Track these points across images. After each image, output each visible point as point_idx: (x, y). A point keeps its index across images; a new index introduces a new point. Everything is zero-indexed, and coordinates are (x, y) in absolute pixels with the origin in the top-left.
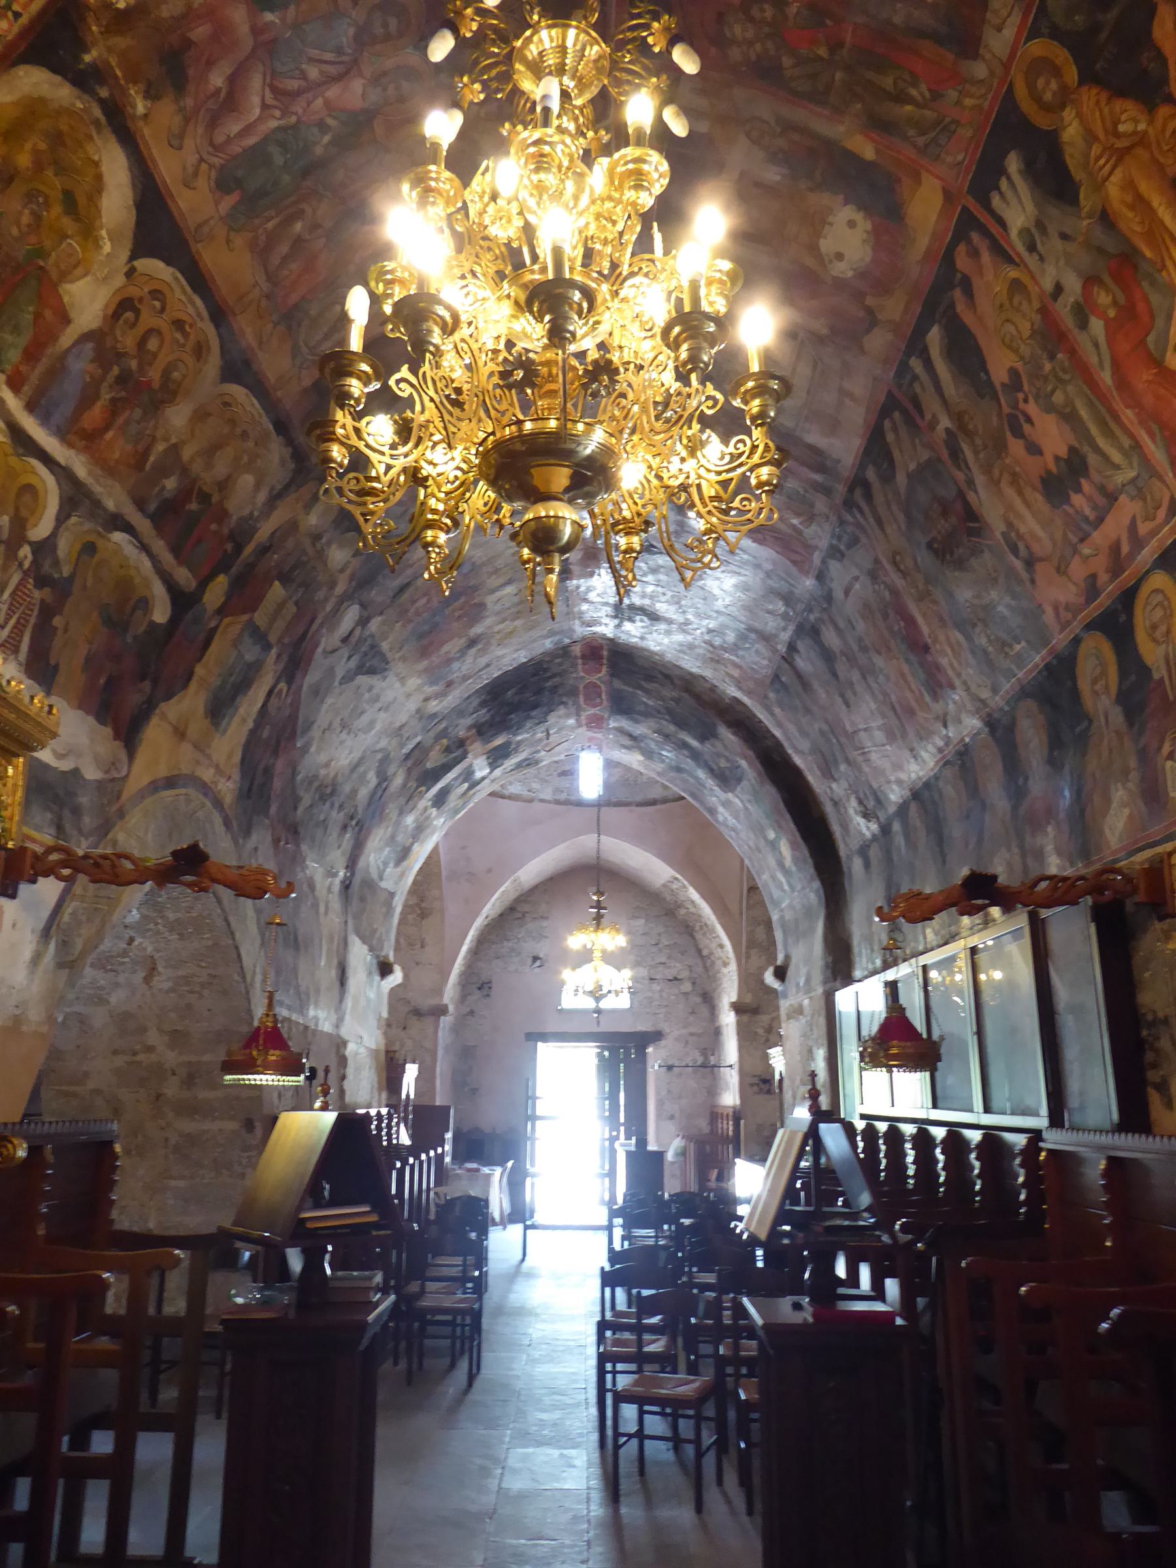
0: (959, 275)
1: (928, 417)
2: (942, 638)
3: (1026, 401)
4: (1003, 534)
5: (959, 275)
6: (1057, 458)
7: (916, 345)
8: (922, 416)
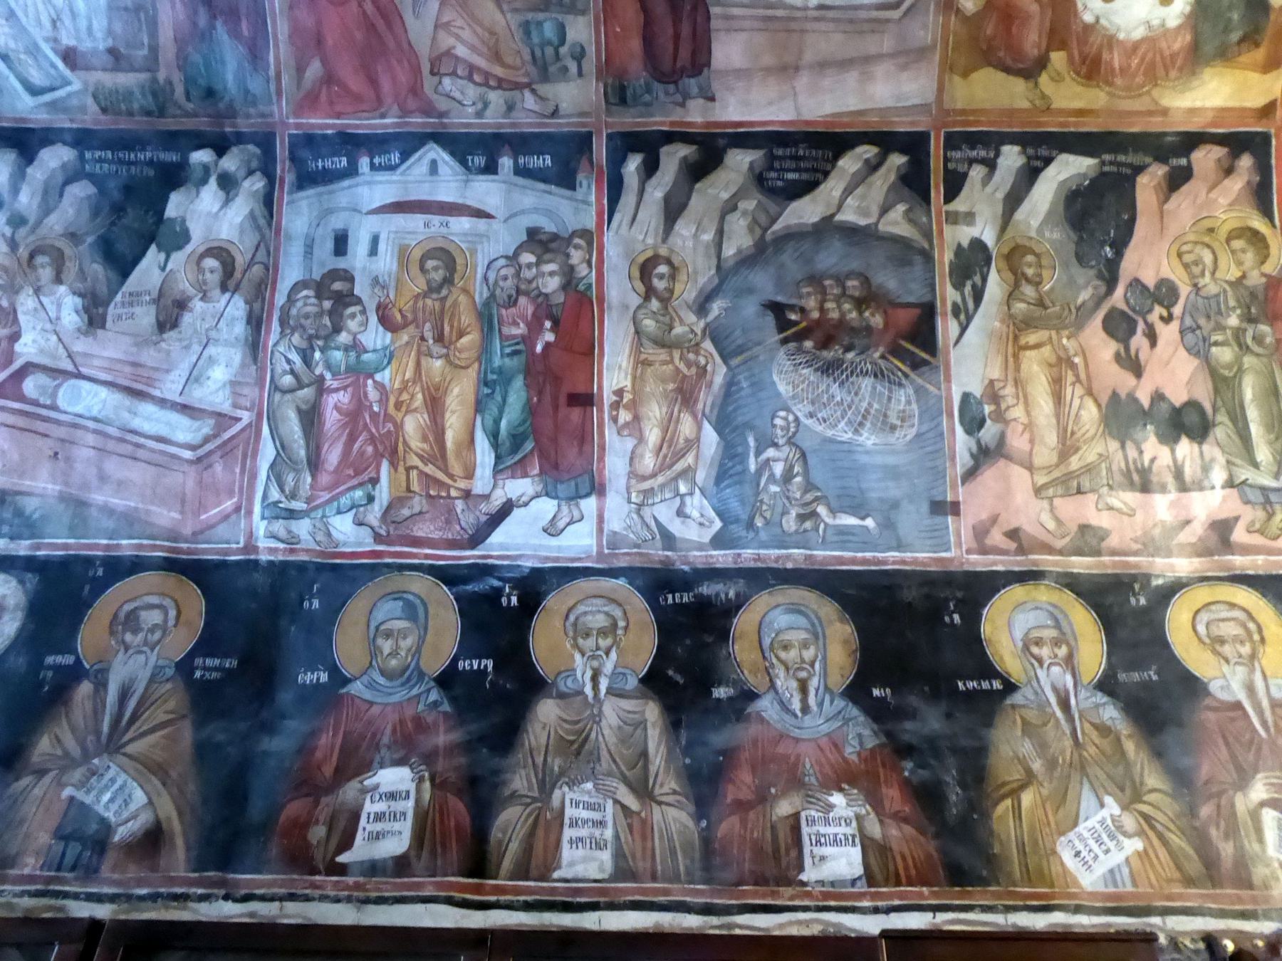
0: (1183, 161)
1: (959, 205)
2: (654, 412)
3: (1167, 320)
4: (966, 397)
5: (1183, 161)
6: (1158, 397)
7: (1042, 146)
8: (950, 197)
